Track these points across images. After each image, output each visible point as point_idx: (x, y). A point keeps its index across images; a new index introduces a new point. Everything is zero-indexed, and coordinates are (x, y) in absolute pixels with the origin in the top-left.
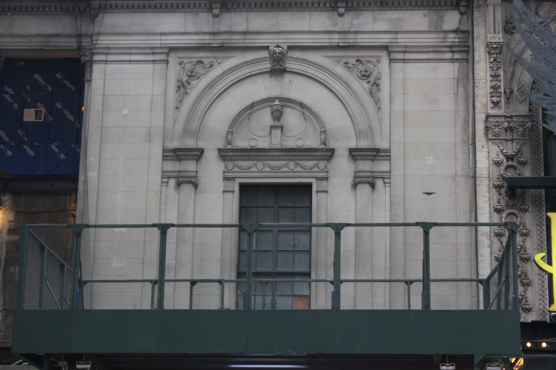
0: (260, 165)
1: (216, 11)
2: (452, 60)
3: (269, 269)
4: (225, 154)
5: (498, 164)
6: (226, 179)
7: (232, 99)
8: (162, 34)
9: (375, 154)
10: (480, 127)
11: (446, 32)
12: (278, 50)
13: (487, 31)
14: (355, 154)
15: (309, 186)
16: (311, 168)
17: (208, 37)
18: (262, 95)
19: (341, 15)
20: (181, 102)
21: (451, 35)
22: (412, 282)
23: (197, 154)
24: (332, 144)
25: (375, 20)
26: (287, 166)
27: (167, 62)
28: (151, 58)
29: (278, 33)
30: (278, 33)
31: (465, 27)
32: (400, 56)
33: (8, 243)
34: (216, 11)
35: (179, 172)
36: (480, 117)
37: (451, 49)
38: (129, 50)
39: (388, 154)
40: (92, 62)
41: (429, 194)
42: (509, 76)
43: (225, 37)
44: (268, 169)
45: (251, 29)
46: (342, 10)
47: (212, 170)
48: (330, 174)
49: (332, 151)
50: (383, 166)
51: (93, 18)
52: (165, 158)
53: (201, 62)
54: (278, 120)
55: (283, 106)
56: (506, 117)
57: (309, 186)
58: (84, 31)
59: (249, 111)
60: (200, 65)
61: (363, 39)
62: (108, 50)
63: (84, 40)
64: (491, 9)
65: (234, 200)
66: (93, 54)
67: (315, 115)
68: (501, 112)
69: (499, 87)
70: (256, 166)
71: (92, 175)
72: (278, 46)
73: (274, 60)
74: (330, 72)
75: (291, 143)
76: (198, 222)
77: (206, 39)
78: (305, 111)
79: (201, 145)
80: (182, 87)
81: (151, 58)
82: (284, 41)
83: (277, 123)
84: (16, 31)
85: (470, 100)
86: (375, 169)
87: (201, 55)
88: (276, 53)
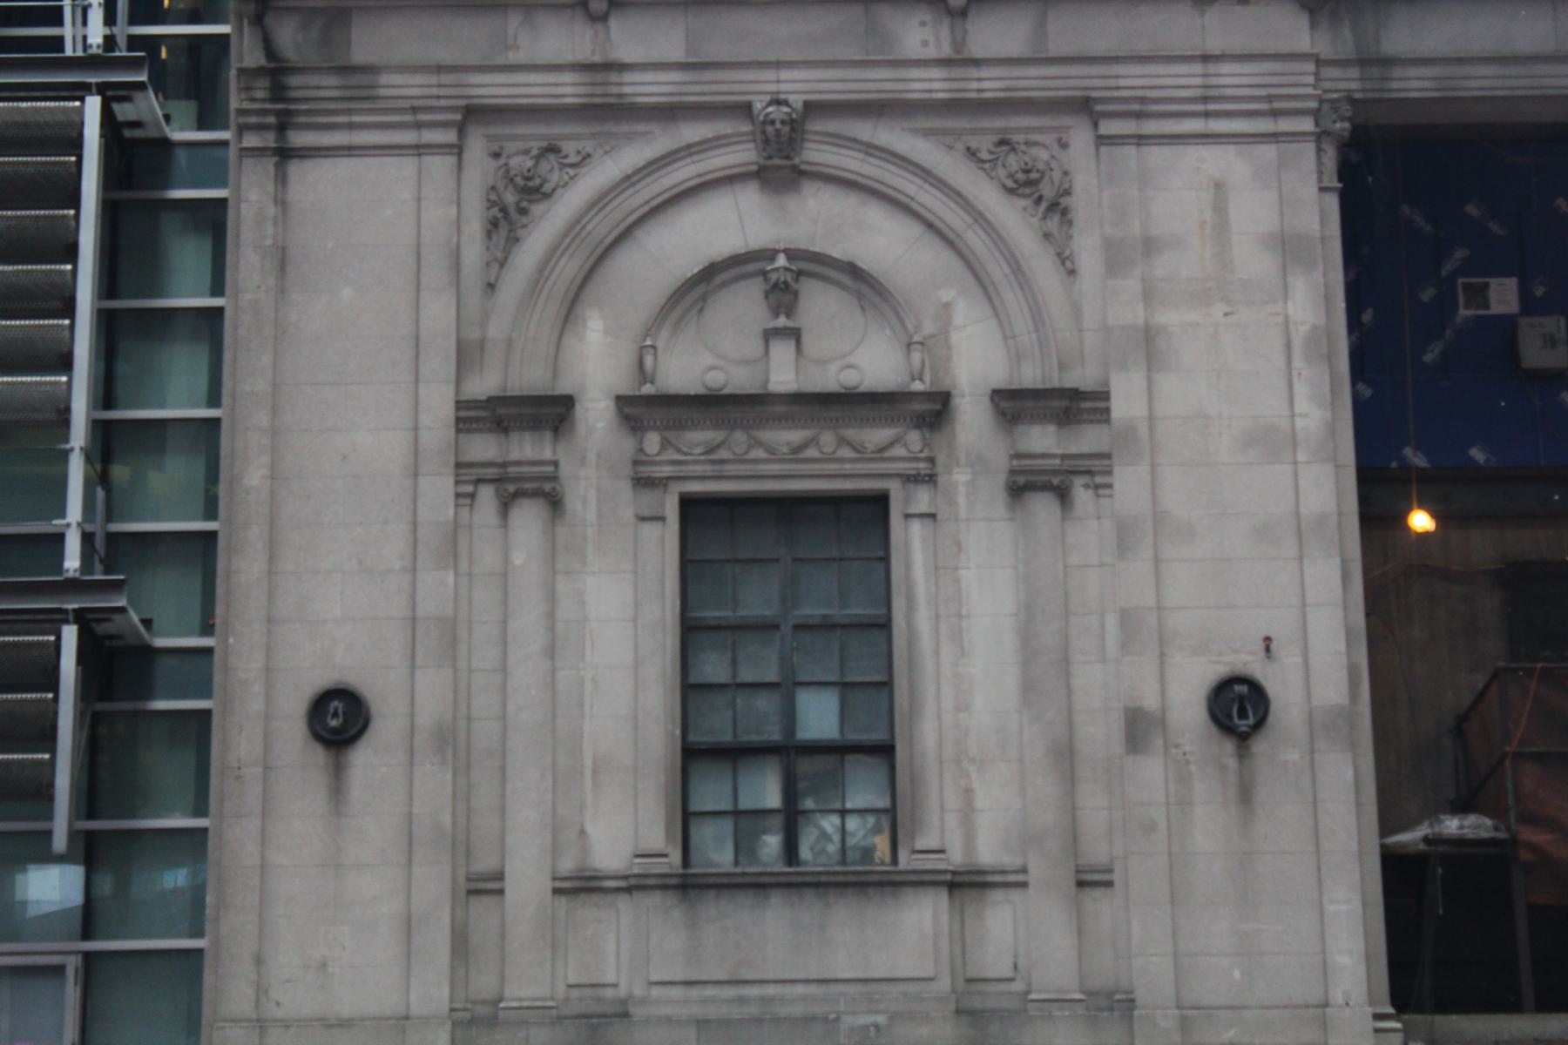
16: (798, 449)
35: (504, 465)
39: (1100, 405)
54: (788, 316)
55: (800, 274)
59: (701, 289)
60: (552, 157)
72: (778, 102)
73: (767, 141)
78: (864, 288)
83: (782, 321)
88: (773, 122)
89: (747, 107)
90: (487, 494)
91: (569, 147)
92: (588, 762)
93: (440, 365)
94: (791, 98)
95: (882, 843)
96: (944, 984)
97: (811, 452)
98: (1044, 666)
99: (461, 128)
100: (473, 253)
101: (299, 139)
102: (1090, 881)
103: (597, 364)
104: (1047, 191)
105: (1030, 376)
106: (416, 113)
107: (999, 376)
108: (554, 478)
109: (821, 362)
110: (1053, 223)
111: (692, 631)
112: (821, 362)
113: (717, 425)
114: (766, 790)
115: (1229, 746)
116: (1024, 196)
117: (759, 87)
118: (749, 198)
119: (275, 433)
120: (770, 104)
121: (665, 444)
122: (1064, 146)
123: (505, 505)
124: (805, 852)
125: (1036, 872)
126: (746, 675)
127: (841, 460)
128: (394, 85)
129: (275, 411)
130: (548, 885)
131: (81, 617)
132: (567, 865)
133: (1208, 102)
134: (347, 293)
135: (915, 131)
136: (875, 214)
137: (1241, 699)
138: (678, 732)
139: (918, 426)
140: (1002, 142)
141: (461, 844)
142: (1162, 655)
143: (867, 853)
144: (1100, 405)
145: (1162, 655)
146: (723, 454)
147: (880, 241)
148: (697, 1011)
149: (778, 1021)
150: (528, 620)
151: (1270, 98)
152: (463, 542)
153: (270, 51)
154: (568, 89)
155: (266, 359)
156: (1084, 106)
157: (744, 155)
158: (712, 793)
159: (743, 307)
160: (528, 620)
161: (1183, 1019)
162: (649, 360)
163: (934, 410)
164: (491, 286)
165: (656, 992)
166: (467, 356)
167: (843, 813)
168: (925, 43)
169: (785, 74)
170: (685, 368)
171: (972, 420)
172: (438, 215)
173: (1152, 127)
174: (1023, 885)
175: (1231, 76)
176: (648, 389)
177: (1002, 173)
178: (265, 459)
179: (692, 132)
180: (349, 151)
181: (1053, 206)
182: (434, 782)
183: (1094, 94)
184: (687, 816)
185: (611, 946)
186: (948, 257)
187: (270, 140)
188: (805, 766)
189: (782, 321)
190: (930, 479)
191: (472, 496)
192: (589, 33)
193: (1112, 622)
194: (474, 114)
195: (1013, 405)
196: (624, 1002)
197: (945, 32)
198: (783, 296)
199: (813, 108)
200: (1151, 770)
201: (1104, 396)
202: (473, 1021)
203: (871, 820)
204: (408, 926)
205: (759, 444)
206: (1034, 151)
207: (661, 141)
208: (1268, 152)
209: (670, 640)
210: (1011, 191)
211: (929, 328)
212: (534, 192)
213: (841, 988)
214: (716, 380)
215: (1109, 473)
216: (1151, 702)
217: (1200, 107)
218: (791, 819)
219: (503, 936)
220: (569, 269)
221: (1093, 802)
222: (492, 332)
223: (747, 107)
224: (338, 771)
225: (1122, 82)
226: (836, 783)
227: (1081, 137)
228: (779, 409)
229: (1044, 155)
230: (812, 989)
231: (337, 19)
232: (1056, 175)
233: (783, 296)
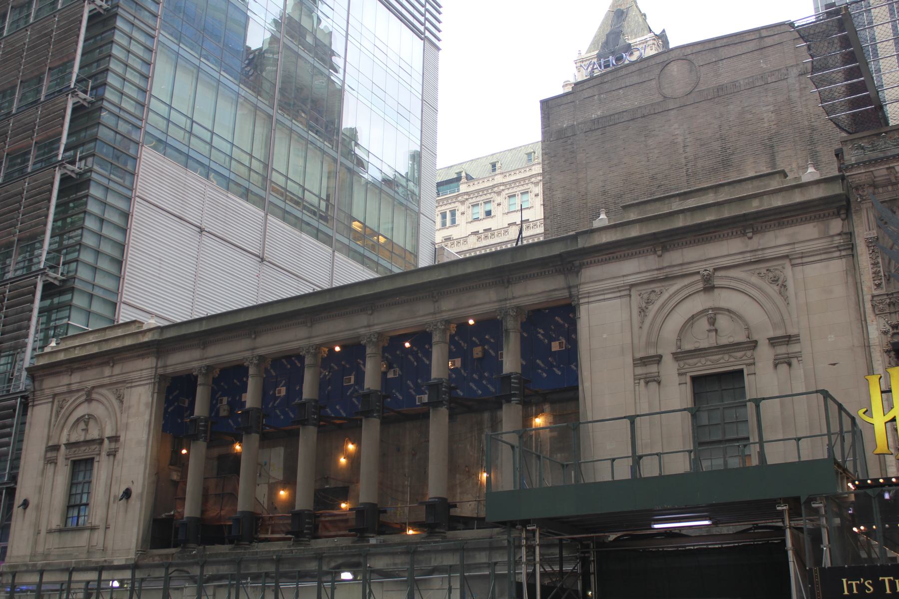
0: (703, 360)
1: (659, 253)
2: (840, 257)
3: (720, 438)
4: (678, 356)
5: (885, 333)
6: (680, 374)
7: (679, 313)
8: (624, 276)
9: (789, 339)
10: (868, 306)
11: (832, 236)
12: (705, 273)
13: (864, 229)
14: (774, 342)
15: (741, 372)
17: (656, 272)
18: (700, 308)
19: (750, 238)
20: (643, 322)
21: (837, 238)
22: (799, 439)
23: (658, 359)
24: (755, 337)
25: (776, 237)
26: (723, 358)
27: (630, 296)
28: (618, 294)
29: (705, 260)
30: (705, 260)
31: (846, 230)
32: (799, 261)
33: (551, 438)
34: (659, 253)
36: (868, 298)
37: (838, 248)
38: (603, 292)
40: (579, 305)
41: (834, 364)
42: (887, 261)
43: (668, 270)
44: (709, 363)
45: (686, 260)
46: (750, 235)
47: (669, 369)
48: (756, 360)
49: (756, 342)
50: (794, 348)
51: (577, 273)
52: (635, 365)
53: (654, 291)
56: (887, 295)
57: (741, 372)
58: (571, 284)
61: (769, 254)
62: (589, 295)
63: (572, 290)
64: (864, 213)
65: (688, 389)
66: (579, 299)
67: (740, 317)
68: (883, 291)
69: (879, 272)
70: (723, 358)
71: (587, 384)
74: (748, 283)
75: (724, 341)
76: (663, 410)
77: (655, 274)
79: (660, 352)
80: (643, 311)
81: (618, 294)
82: (710, 266)
84: (529, 291)
85: (857, 287)
86: (790, 351)
87: (653, 286)
89: (82, 390)
93: (45, 441)
101: (36, 403)
118: (86, 405)
128: (47, 392)
131: (7, 488)
136: (100, 406)
154: (65, 389)
156: (124, 382)
163: (101, 441)
166: (49, 438)
170: (73, 439)
179: (80, 394)
184: (67, 518)
194: (55, 396)
199: (93, 388)
212: (62, 408)
220: (63, 421)
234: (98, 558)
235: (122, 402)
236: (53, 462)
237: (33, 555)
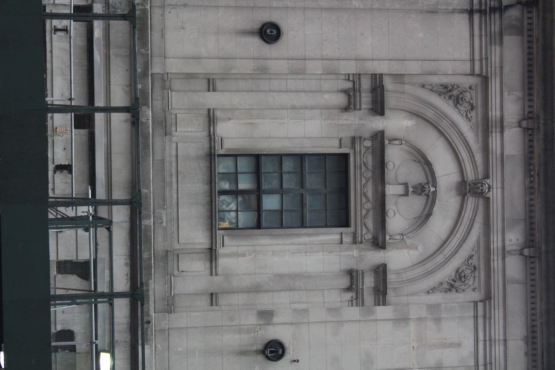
35: (360, 91)
39: (381, 303)
54: (412, 191)
59: (422, 161)
60: (470, 107)
72: (489, 188)
73: (475, 184)
78: (423, 218)
83: (411, 189)
88: (482, 186)
90: (349, 85)
91: (473, 114)
92: (254, 121)
93: (396, 68)
94: (491, 193)
95: (226, 225)
96: (177, 247)
97: (364, 200)
98: (289, 282)
99: (480, 75)
100: (435, 80)
101: (476, 17)
102: (213, 298)
103: (395, 123)
104: (458, 284)
105: (391, 277)
106: (485, 59)
107: (391, 266)
108: (355, 109)
109: (396, 204)
110: (446, 286)
111: (301, 157)
112: (396, 204)
113: (373, 166)
114: (245, 184)
115: (260, 347)
116: (456, 275)
117: (495, 181)
118: (455, 178)
119: (371, 9)
120: (489, 185)
121: (367, 148)
122: (474, 290)
123: (345, 92)
124: (223, 197)
125: (215, 278)
126: (285, 177)
127: (361, 210)
128: (496, 51)
129: (379, 10)
130: (211, 107)
132: (218, 114)
133: (489, 341)
134: (421, 35)
135: (479, 237)
136: (449, 223)
137: (277, 352)
138: (265, 153)
139: (373, 238)
140: (475, 268)
141: (226, 76)
142: (292, 324)
143: (223, 220)
144: (381, 303)
145: (292, 324)
146: (364, 169)
147: (440, 224)
148: (167, 159)
149: (164, 188)
150: (304, 99)
151: (491, 363)
152: (332, 77)
153: (508, 7)
154: (494, 113)
155: (397, 6)
156: (488, 297)
157: (470, 176)
158: (244, 164)
159: (416, 176)
160: (304, 99)
161: (165, 330)
162: (397, 142)
163: (379, 243)
164: (423, 86)
165: (174, 145)
166: (399, 77)
167: (237, 211)
168: (511, 240)
169: (499, 191)
170: (394, 155)
171: (376, 257)
172: (449, 67)
173: (480, 321)
174: (211, 275)
175: (499, 350)
176: (386, 142)
177: (464, 268)
178: (362, 6)
180: (472, 35)
181: (452, 286)
182: (247, 66)
183: (492, 301)
184: (236, 156)
185: (190, 129)
186: (435, 248)
187: (476, 7)
188: (253, 198)
189: (411, 189)
190: (355, 242)
191: (349, 80)
192: (514, 121)
193: (304, 306)
194: (485, 80)
195: (381, 271)
196: (170, 134)
197: (515, 248)
198: (420, 189)
200: (252, 320)
201: (384, 304)
202: (164, 81)
203: (234, 221)
204: (197, 58)
205: (367, 181)
206: (472, 279)
207: (475, 146)
208: (472, 363)
209: (298, 150)
210: (457, 271)
211: (408, 242)
212: (457, 101)
213: (175, 210)
214: (390, 166)
215: (357, 306)
216: (276, 320)
217: (487, 339)
218: (235, 193)
219: (193, 91)
220: (429, 114)
221: (240, 299)
222: (407, 87)
223: (488, 177)
224: (251, 33)
225: (497, 311)
226: (247, 208)
227: (477, 296)
228: (380, 189)
229: (470, 283)
230: (175, 200)
231: (519, 31)
232: (463, 287)
233: (420, 189)
234: (155, 288)
235: (451, 287)
236: (350, 106)
237: (165, 82)
